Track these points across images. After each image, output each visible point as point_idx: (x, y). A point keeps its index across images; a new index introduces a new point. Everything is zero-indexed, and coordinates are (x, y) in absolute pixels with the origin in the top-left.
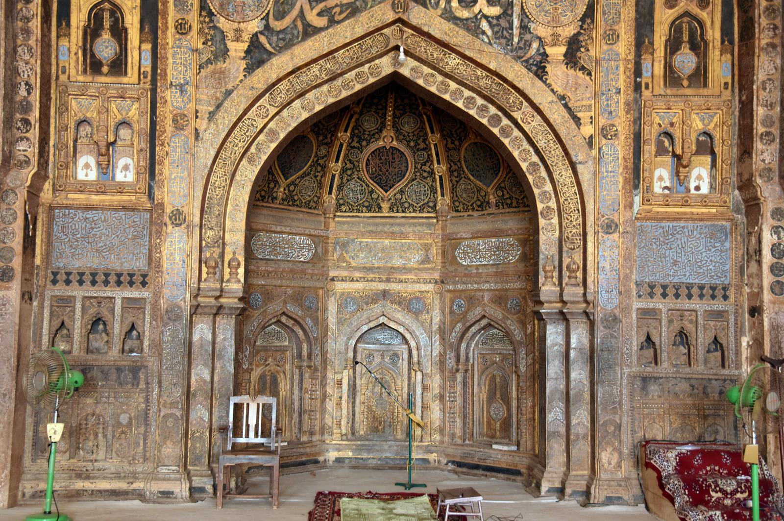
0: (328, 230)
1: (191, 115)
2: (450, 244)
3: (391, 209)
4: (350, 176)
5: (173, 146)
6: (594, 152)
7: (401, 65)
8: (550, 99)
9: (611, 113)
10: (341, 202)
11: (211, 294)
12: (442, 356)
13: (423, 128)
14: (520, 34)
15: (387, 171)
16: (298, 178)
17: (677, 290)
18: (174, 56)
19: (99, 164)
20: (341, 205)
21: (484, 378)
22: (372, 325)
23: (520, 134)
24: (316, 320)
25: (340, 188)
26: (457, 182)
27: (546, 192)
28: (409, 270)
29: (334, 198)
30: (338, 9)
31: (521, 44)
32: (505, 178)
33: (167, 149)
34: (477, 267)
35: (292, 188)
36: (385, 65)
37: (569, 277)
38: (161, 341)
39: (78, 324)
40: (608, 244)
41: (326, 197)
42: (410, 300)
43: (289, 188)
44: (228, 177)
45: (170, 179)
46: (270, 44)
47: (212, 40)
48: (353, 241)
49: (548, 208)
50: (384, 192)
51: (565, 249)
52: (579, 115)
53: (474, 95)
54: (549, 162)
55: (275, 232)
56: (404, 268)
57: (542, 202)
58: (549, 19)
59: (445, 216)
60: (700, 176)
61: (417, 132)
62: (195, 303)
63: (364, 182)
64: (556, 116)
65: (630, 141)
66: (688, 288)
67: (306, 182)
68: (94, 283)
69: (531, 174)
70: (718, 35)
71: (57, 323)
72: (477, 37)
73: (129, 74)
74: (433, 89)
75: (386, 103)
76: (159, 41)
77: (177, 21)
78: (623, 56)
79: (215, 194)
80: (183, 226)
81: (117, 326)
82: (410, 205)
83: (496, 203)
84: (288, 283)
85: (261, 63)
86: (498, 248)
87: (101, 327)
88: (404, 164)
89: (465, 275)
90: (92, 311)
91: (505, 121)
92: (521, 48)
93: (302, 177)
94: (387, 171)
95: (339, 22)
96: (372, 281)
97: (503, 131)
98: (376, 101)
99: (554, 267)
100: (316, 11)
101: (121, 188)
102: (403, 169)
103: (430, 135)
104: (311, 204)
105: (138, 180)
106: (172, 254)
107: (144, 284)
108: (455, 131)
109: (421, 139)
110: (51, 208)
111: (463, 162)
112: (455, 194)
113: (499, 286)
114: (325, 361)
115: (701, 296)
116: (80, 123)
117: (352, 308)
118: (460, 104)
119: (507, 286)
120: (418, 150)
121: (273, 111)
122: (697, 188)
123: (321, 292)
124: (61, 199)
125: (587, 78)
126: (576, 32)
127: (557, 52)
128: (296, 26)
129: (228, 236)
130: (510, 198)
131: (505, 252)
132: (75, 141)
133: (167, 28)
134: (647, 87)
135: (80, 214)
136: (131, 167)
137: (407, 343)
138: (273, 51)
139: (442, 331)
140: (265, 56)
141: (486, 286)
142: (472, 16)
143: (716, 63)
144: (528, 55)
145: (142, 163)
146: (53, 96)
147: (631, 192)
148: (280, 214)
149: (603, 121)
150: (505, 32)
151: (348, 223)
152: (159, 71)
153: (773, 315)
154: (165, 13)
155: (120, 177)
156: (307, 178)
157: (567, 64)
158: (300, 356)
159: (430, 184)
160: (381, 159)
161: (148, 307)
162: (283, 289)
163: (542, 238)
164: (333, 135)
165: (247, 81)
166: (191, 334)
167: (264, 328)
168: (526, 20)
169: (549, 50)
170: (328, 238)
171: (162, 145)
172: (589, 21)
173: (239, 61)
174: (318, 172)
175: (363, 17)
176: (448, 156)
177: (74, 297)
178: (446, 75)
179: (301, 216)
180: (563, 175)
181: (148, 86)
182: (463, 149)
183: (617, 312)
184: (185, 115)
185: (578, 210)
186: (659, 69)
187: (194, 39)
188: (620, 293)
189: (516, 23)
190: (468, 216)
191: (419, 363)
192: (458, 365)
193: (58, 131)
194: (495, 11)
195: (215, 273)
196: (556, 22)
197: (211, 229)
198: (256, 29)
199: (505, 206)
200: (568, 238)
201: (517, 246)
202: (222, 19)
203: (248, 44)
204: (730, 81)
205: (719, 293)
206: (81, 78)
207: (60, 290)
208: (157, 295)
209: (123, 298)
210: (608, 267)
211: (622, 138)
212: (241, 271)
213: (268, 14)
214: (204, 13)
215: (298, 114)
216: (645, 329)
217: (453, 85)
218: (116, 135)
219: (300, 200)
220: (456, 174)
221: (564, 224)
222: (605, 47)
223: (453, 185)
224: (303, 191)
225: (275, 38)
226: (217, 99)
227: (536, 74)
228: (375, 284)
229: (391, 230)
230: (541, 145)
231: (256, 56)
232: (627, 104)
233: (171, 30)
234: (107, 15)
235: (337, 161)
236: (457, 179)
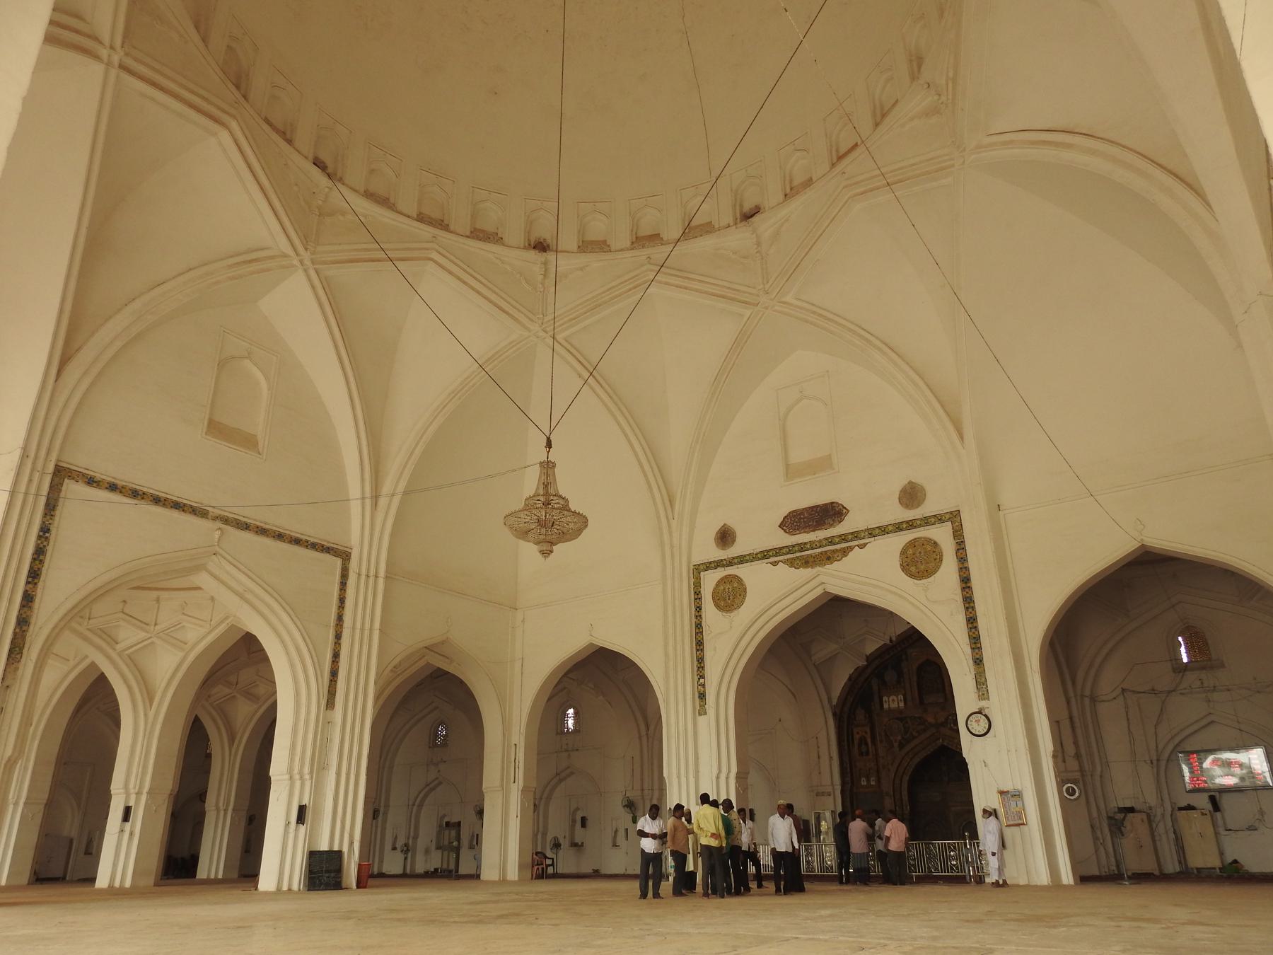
215: (917, 760)
231: (901, 746)
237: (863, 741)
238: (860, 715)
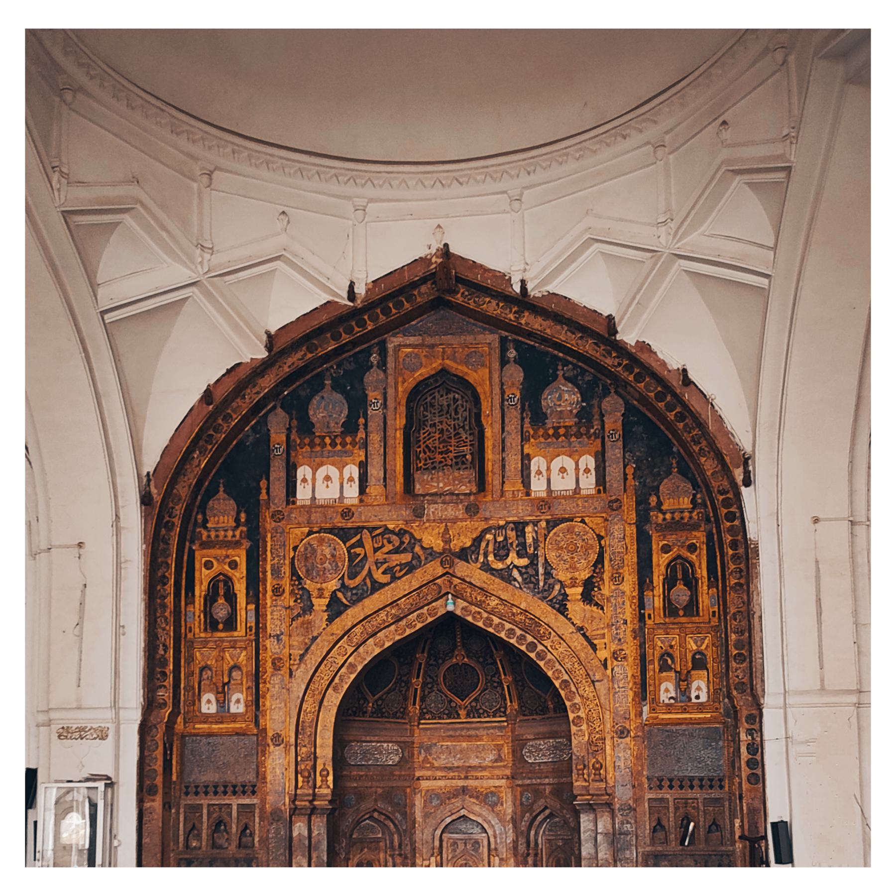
0: (413, 736)
2: (518, 745)
5: (274, 684)
6: (609, 672)
8: (571, 630)
9: (620, 640)
11: (306, 798)
12: (515, 842)
17: (681, 782)
18: (272, 614)
19: (218, 701)
21: (551, 860)
22: (454, 817)
24: (404, 815)
28: (484, 768)
30: (398, 568)
31: (546, 587)
33: (268, 685)
37: (595, 774)
38: (267, 838)
39: (205, 826)
42: (487, 794)
44: (317, 705)
45: (271, 709)
48: (435, 744)
49: (578, 717)
52: (595, 642)
53: (514, 627)
56: (480, 767)
57: (573, 712)
58: (568, 566)
60: (700, 688)
62: (293, 806)
64: (576, 644)
65: (638, 661)
66: (690, 780)
68: (216, 793)
69: (563, 689)
70: (705, 573)
71: (190, 826)
73: (239, 629)
78: (628, 593)
79: (307, 718)
80: (282, 746)
81: (234, 826)
85: (339, 614)
86: (555, 747)
87: (222, 827)
89: (530, 772)
90: (215, 815)
91: (540, 647)
92: (545, 591)
95: (400, 578)
100: (380, 571)
101: (235, 717)
105: (247, 711)
107: (254, 792)
110: (183, 736)
113: (556, 781)
114: (414, 850)
115: (701, 787)
116: (202, 669)
117: (435, 802)
122: (698, 697)
123: (408, 790)
124: (190, 730)
125: (601, 612)
127: (575, 592)
128: (365, 584)
131: (560, 751)
132: (199, 684)
133: (266, 591)
134: (650, 617)
135: (204, 740)
136: (242, 701)
137: (486, 832)
139: (514, 821)
141: (547, 781)
143: (705, 596)
145: (250, 698)
146: (183, 650)
147: (640, 703)
153: (750, 801)
154: (265, 580)
155: (234, 709)
158: (392, 847)
161: (257, 811)
162: (374, 789)
165: (328, 629)
166: (291, 831)
167: (358, 823)
170: (413, 743)
172: (600, 566)
175: (418, 572)
177: (202, 805)
181: (253, 637)
183: (631, 802)
186: (658, 603)
188: (634, 786)
191: (496, 849)
192: (528, 850)
193: (186, 678)
194: (524, 562)
195: (308, 782)
196: (573, 568)
197: (305, 746)
198: (335, 588)
202: (308, 582)
204: (717, 610)
205: (716, 783)
206: (203, 635)
207: (191, 800)
208: (263, 801)
209: (238, 805)
210: (622, 765)
211: (630, 660)
212: (330, 778)
214: (294, 578)
215: (372, 650)
216: (656, 815)
218: (230, 676)
222: (613, 587)
225: (349, 594)
226: (306, 644)
227: (559, 611)
228: (454, 781)
231: (335, 609)
232: (634, 631)
233: (269, 593)
234: (221, 585)
237: (221, 588)
238: (223, 516)
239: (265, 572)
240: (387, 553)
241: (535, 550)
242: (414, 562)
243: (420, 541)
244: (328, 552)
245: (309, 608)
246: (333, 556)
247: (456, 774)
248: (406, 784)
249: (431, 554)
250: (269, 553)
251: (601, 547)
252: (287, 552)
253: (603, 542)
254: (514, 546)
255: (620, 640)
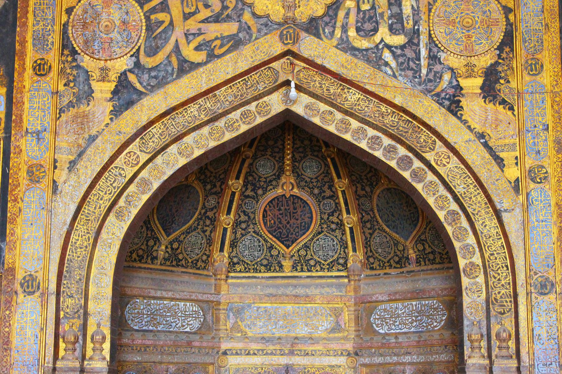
0: (219, 293)
1: (48, 165)
3: (294, 268)
4: (244, 230)
7: (294, 102)
8: (467, 137)
9: (538, 152)
10: (235, 260)
13: (327, 173)
14: (429, 65)
15: (288, 223)
16: (183, 234)
18: (30, 100)
20: (234, 264)
23: (435, 179)
25: (233, 245)
26: (371, 234)
27: (468, 245)
29: (227, 255)
30: (218, 42)
31: (431, 76)
32: (425, 229)
34: (396, 336)
35: (175, 245)
36: (275, 104)
37: (500, 348)
40: (544, 306)
41: (216, 255)
43: (172, 245)
44: (92, 236)
46: (141, 83)
47: (74, 80)
48: (249, 306)
49: (472, 264)
50: (285, 248)
51: (493, 313)
52: (502, 155)
54: (469, 210)
55: (154, 298)
56: (311, 338)
58: (462, 48)
59: (358, 275)
61: (321, 177)
63: (261, 236)
64: (474, 157)
67: (193, 237)
69: (450, 224)
72: (379, 69)
74: (332, 129)
75: (283, 145)
76: (15, 84)
77: (36, 62)
79: (77, 254)
80: (37, 294)
82: (317, 262)
83: (417, 259)
84: (170, 358)
85: (130, 104)
88: (307, 215)
89: (383, 346)
91: (417, 164)
92: (430, 81)
93: (188, 232)
94: (288, 223)
95: (219, 56)
96: (272, 354)
97: (415, 174)
98: (271, 143)
99: (482, 336)
102: (307, 220)
103: (336, 180)
104: (199, 264)
106: (22, 328)
108: (365, 176)
109: (327, 186)
111: (376, 211)
112: (369, 249)
113: (422, 359)
118: (363, 145)
119: (432, 358)
120: (324, 198)
121: (144, 157)
123: (211, 368)
125: (509, 113)
126: (493, 61)
127: (473, 84)
128: (170, 62)
129: (91, 306)
130: (432, 253)
131: (428, 317)
133: (25, 69)
138: (143, 90)
140: (135, 97)
141: (408, 359)
142: (372, 46)
144: (438, 90)
148: (161, 277)
149: (530, 162)
150: (411, 63)
151: (243, 285)
152: (14, 117)
156: (194, 233)
157: (484, 97)
159: (339, 238)
160: (280, 210)
162: (164, 366)
163: (466, 300)
164: (223, 183)
165: (113, 125)
168: (435, 50)
169: (463, 83)
170: (219, 303)
171: (15, 200)
173: (105, 103)
174: (206, 226)
176: (359, 205)
178: (346, 112)
179: (186, 278)
180: (487, 224)
182: (376, 197)
184: (41, 166)
185: (507, 266)
187: (53, 81)
189: (424, 53)
190: (385, 274)
194: (399, 40)
197: (71, 296)
198: (125, 67)
199: (427, 262)
200: (496, 299)
201: (443, 310)
202: (87, 58)
203: (115, 84)
210: (544, 335)
212: (107, 346)
213: (138, 50)
214: (66, 52)
215: (174, 160)
217: (355, 124)
219: (186, 259)
220: (368, 225)
221: (490, 283)
222: (527, 78)
223: (366, 239)
224: (189, 249)
225: (146, 76)
226: (79, 146)
227: (449, 109)
228: (275, 358)
229: (294, 292)
230: (459, 190)
233: (29, 72)
235: (229, 213)
236: (371, 231)
239: (23, 42)
240: (203, 22)
241: (416, 23)
242: (241, 35)
243: (251, 6)
244: (116, 16)
245: (88, 95)
246: (124, 23)
247: (278, 347)
248: (208, 360)
249: (266, 23)
250: (30, 16)
251: (509, 23)
252: (57, 14)
253: (511, 17)
254: (385, 18)
255: (538, 152)
